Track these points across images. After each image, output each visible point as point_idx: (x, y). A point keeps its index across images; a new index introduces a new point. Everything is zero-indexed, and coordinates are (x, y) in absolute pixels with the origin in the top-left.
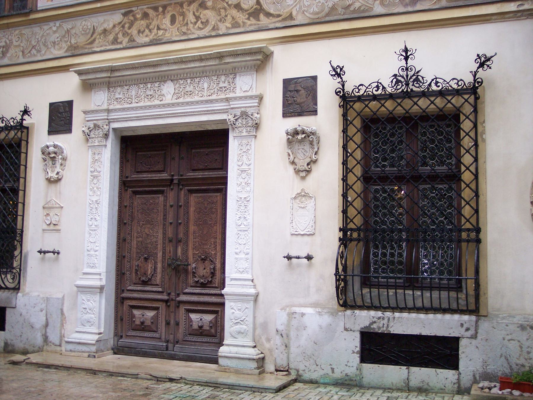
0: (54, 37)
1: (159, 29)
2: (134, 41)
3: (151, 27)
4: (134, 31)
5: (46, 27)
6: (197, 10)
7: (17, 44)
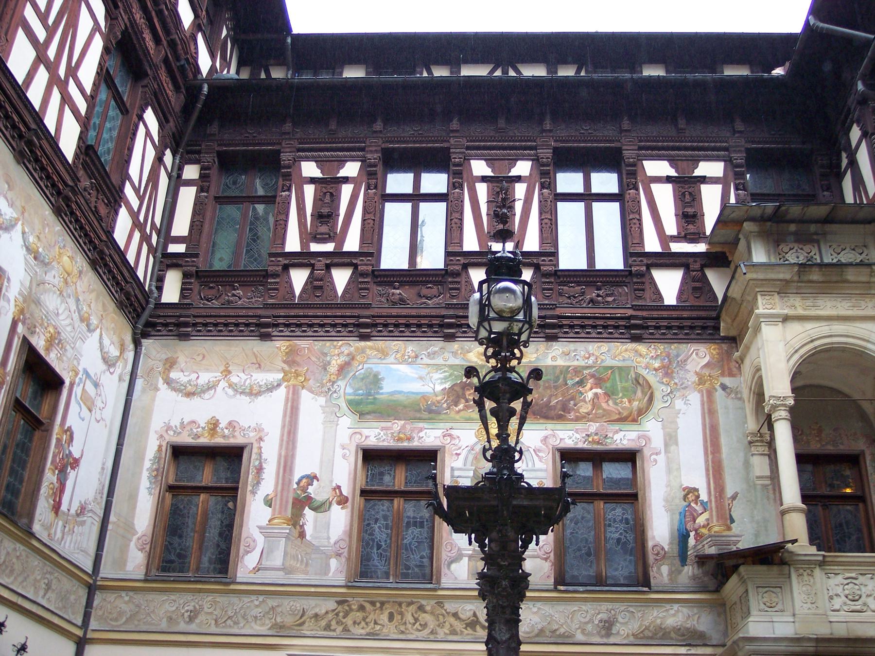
0: (256, 612)
1: (376, 623)
2: (349, 631)
3: (367, 620)
4: (349, 621)
5: (246, 600)
6: (416, 612)
7: (210, 610)
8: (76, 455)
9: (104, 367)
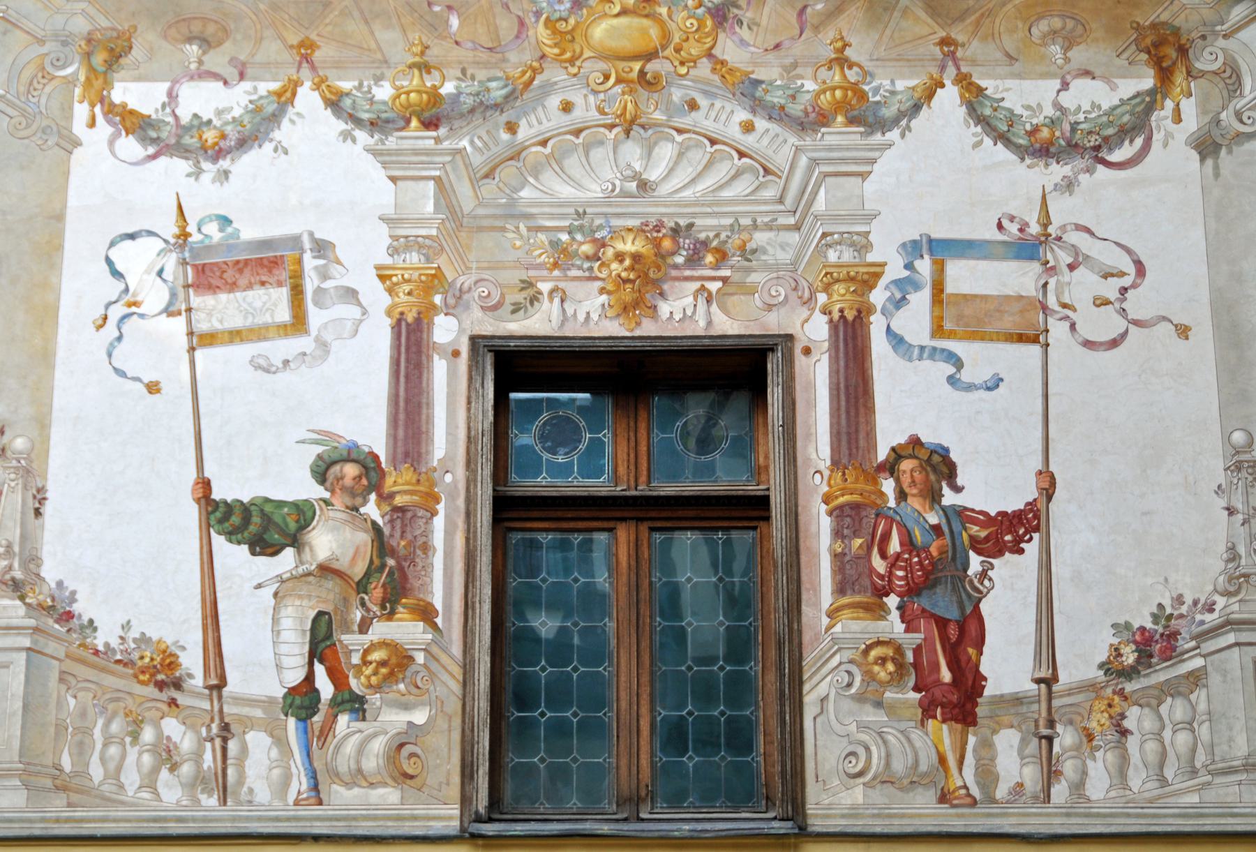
8: (1008, 496)
9: (1058, 171)
